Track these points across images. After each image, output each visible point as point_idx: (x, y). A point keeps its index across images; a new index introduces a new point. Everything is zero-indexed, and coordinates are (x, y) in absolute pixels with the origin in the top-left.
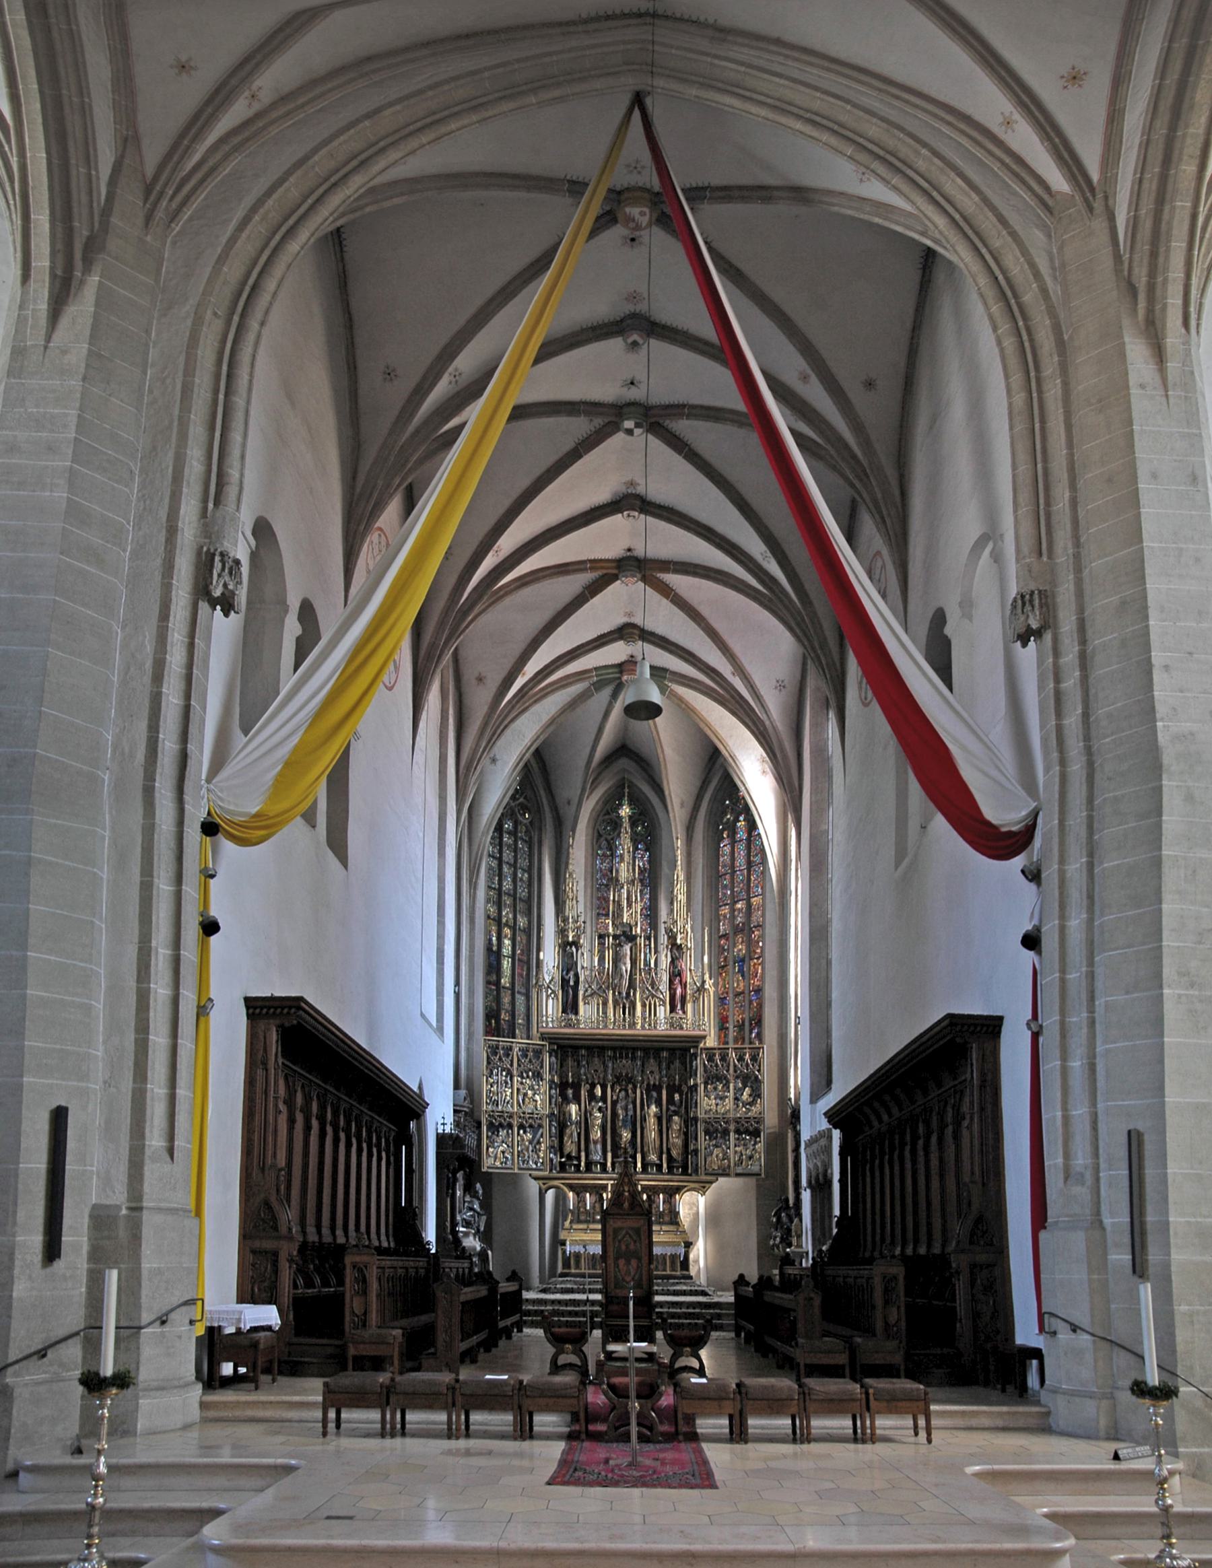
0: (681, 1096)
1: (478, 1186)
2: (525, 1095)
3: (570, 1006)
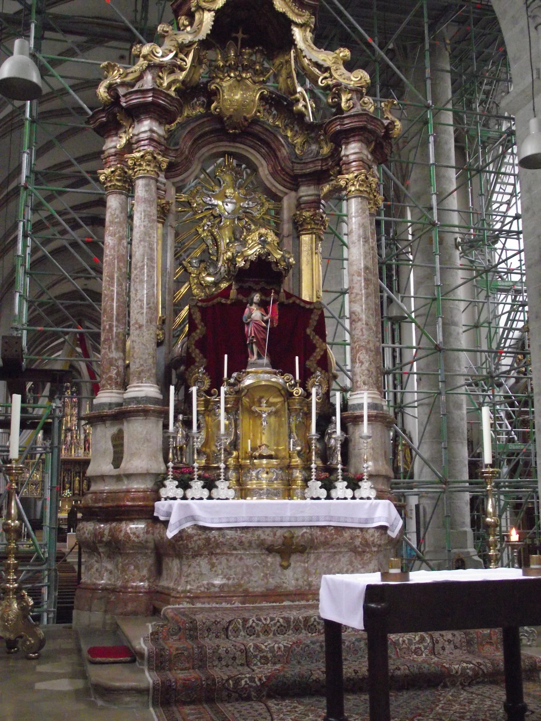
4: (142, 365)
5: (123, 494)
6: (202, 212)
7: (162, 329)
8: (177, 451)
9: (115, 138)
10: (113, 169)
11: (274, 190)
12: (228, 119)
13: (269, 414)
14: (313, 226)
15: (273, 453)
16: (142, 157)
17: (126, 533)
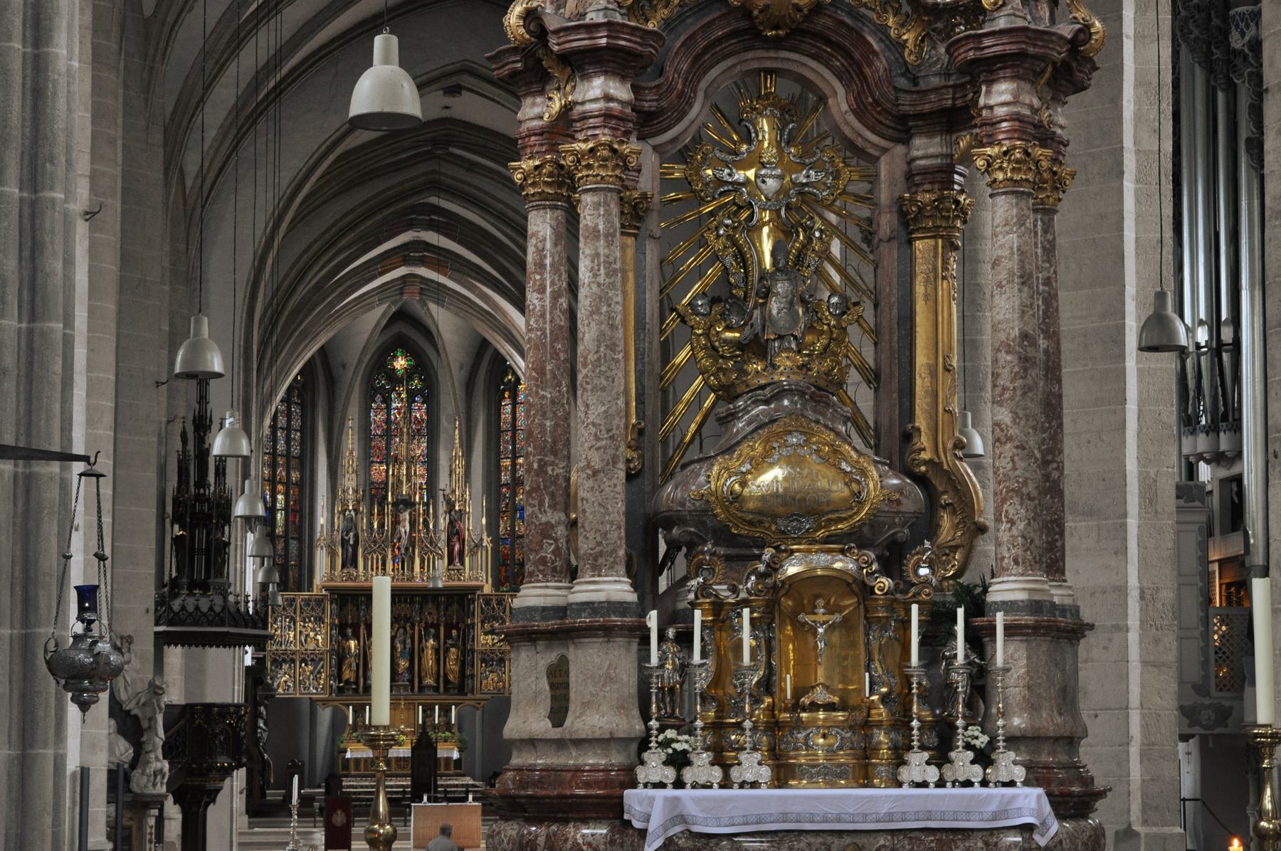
0: (458, 631)
1: (262, 709)
2: (307, 636)
3: (350, 561)
4: (599, 544)
5: (569, 775)
6: (714, 199)
7: (637, 448)
8: (663, 694)
9: (539, 100)
10: (537, 163)
11: (859, 142)
12: (760, 12)
13: (831, 628)
14: (938, 223)
15: (836, 699)
16: (591, 150)
17: (576, 843)
